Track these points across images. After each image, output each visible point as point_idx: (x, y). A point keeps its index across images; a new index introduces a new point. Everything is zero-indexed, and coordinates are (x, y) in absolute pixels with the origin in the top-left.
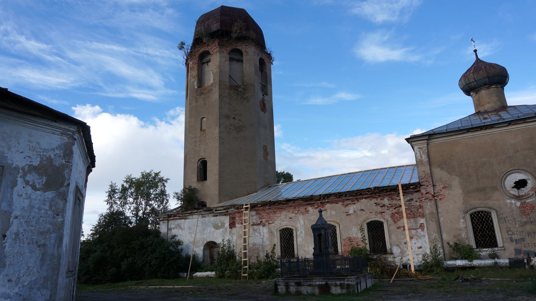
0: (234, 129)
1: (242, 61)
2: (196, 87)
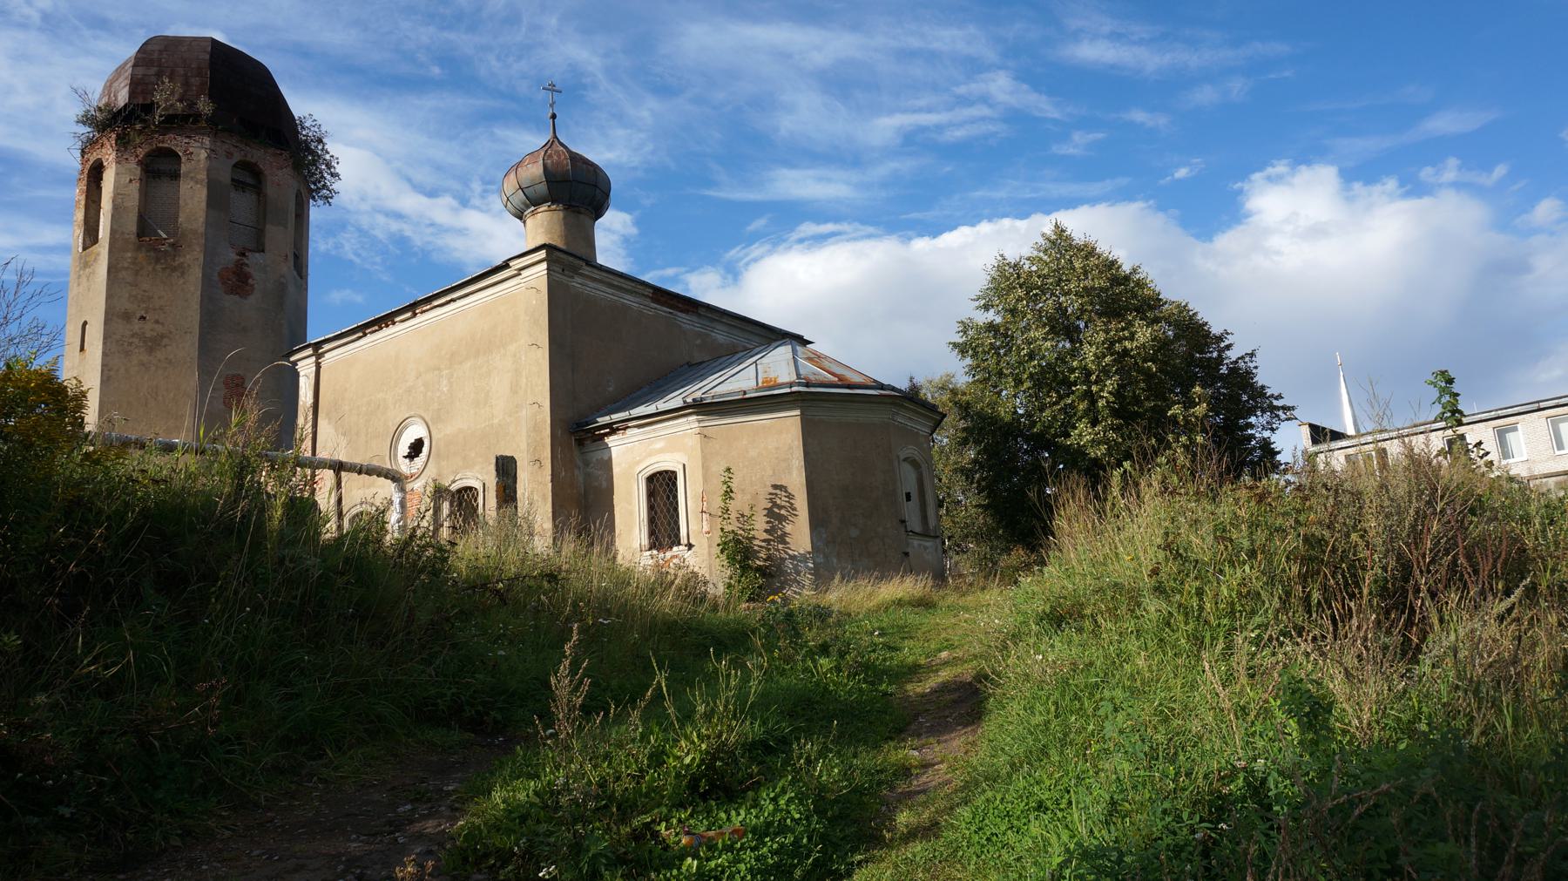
0: (141, 344)
2: (80, 250)
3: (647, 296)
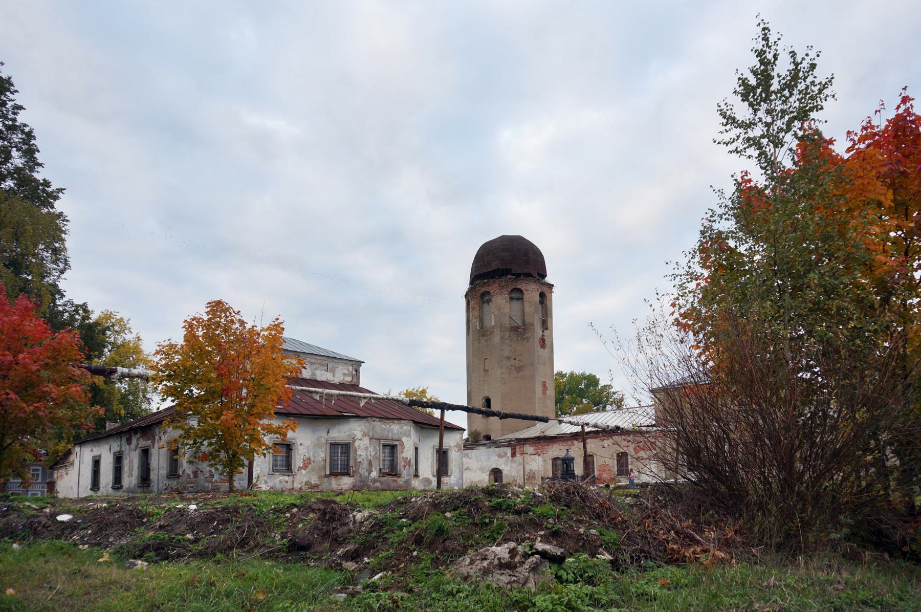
1: (522, 299)
2: (478, 328)
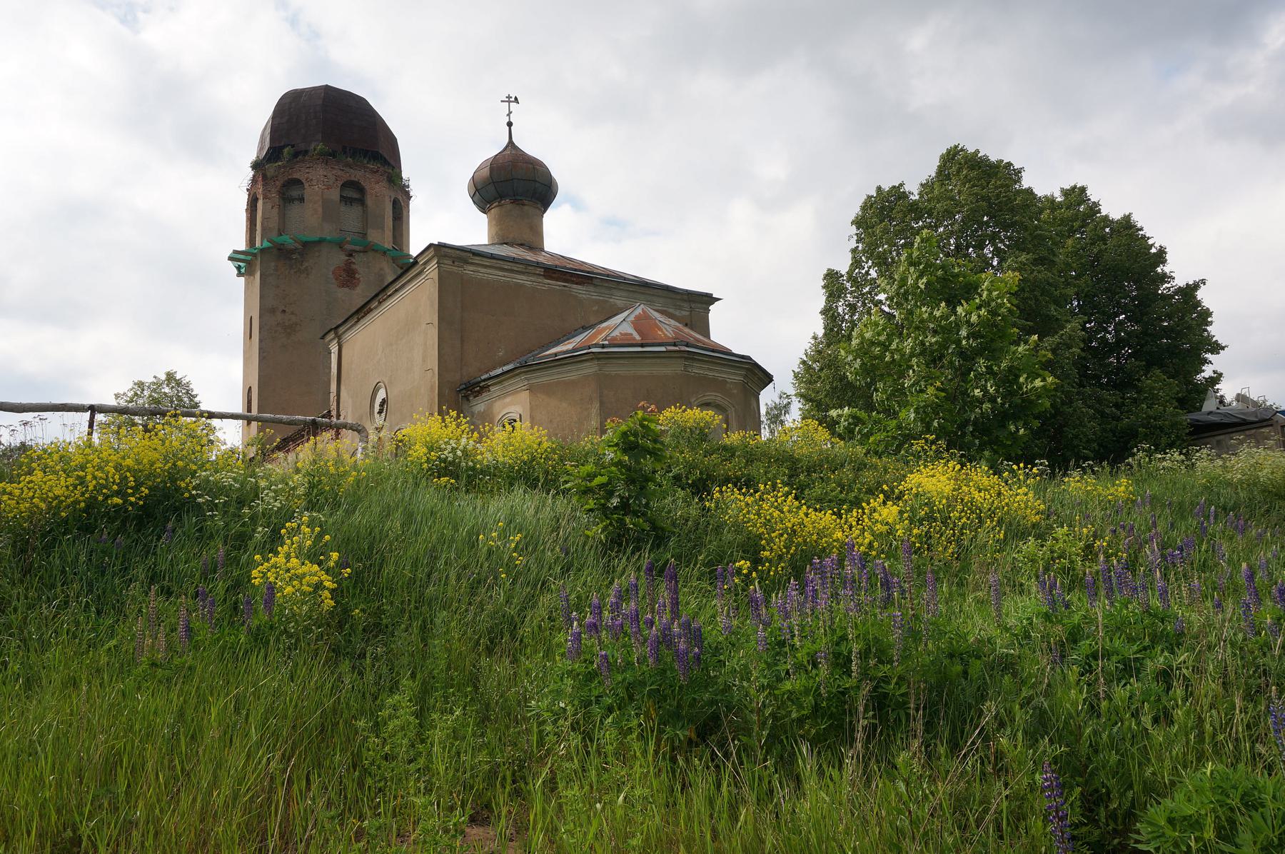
3: (539, 275)
